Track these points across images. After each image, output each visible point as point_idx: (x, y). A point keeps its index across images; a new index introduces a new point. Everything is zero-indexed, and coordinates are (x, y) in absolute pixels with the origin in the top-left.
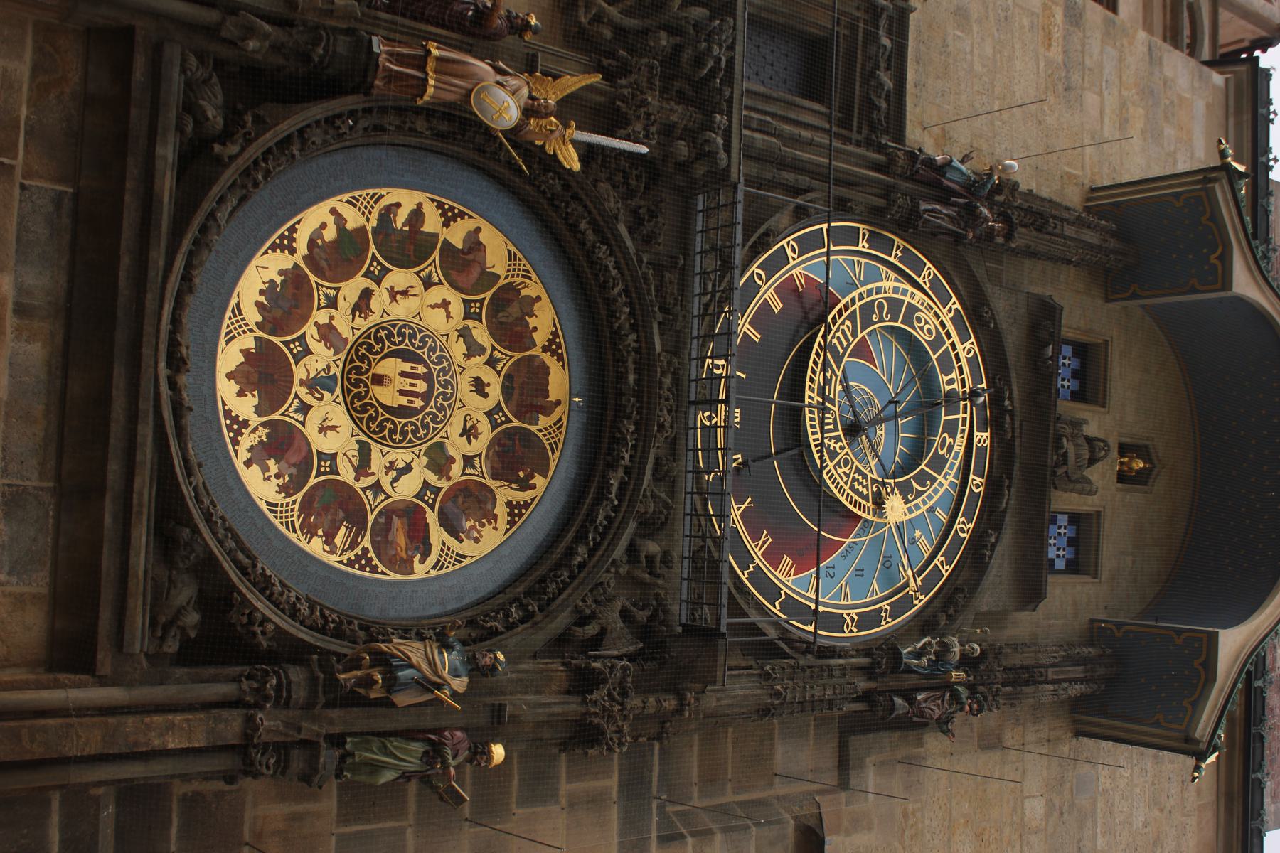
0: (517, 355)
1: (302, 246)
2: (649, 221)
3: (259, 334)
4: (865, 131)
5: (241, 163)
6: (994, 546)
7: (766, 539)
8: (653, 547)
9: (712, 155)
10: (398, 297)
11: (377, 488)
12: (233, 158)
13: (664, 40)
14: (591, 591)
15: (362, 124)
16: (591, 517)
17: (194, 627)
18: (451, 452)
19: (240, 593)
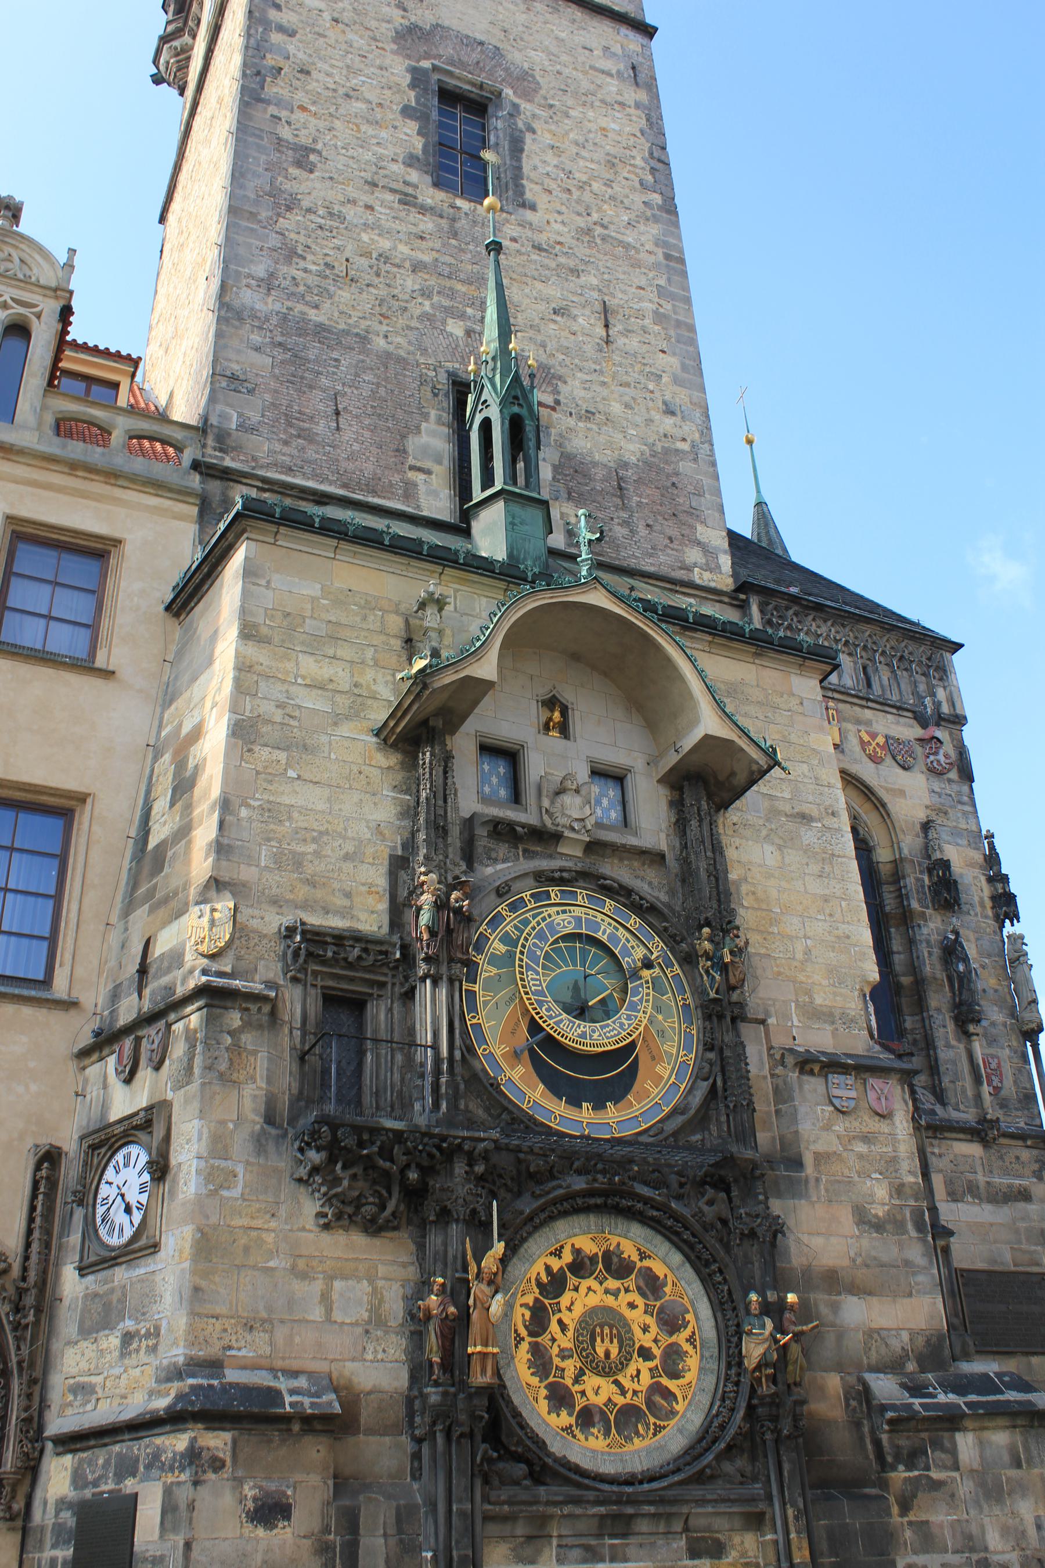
4: (385, 970)
6: (641, 898)
7: (649, 1085)
8: (673, 1179)
12: (540, 1459)
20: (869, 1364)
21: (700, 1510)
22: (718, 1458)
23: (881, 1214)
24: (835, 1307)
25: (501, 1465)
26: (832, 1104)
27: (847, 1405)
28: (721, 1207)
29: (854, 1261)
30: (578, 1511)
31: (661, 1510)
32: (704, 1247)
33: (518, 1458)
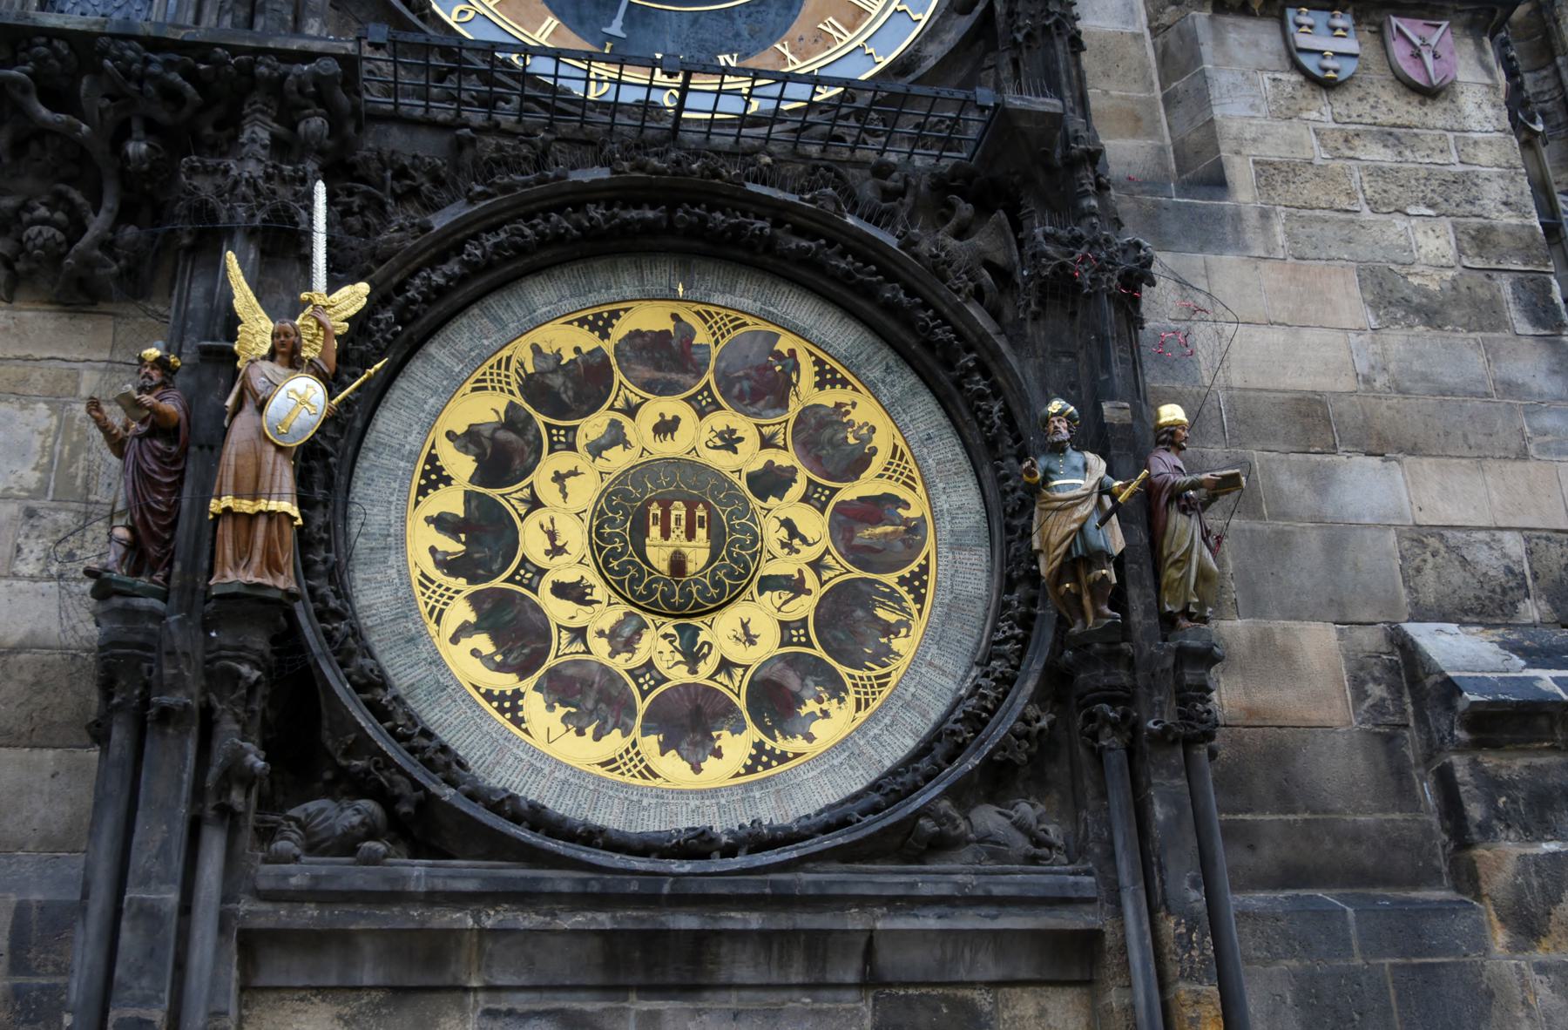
0: (618, 376)
1: (506, 682)
2: (413, 178)
3: (636, 732)
5: (419, 774)
8: (868, 190)
9: (318, 80)
10: (558, 543)
11: (817, 566)
12: (417, 786)
13: (137, 148)
14: (944, 280)
15: (333, 603)
16: (845, 279)
17: (1033, 806)
18: (758, 465)
19: (992, 753)
20: (1416, 604)
21: (900, 923)
22: (956, 793)
23: (1433, 287)
24: (1322, 481)
25: (312, 806)
26: (1298, 67)
27: (1360, 693)
28: (988, 241)
29: (1367, 380)
30: (528, 920)
31: (782, 921)
32: (938, 314)
33: (359, 786)
